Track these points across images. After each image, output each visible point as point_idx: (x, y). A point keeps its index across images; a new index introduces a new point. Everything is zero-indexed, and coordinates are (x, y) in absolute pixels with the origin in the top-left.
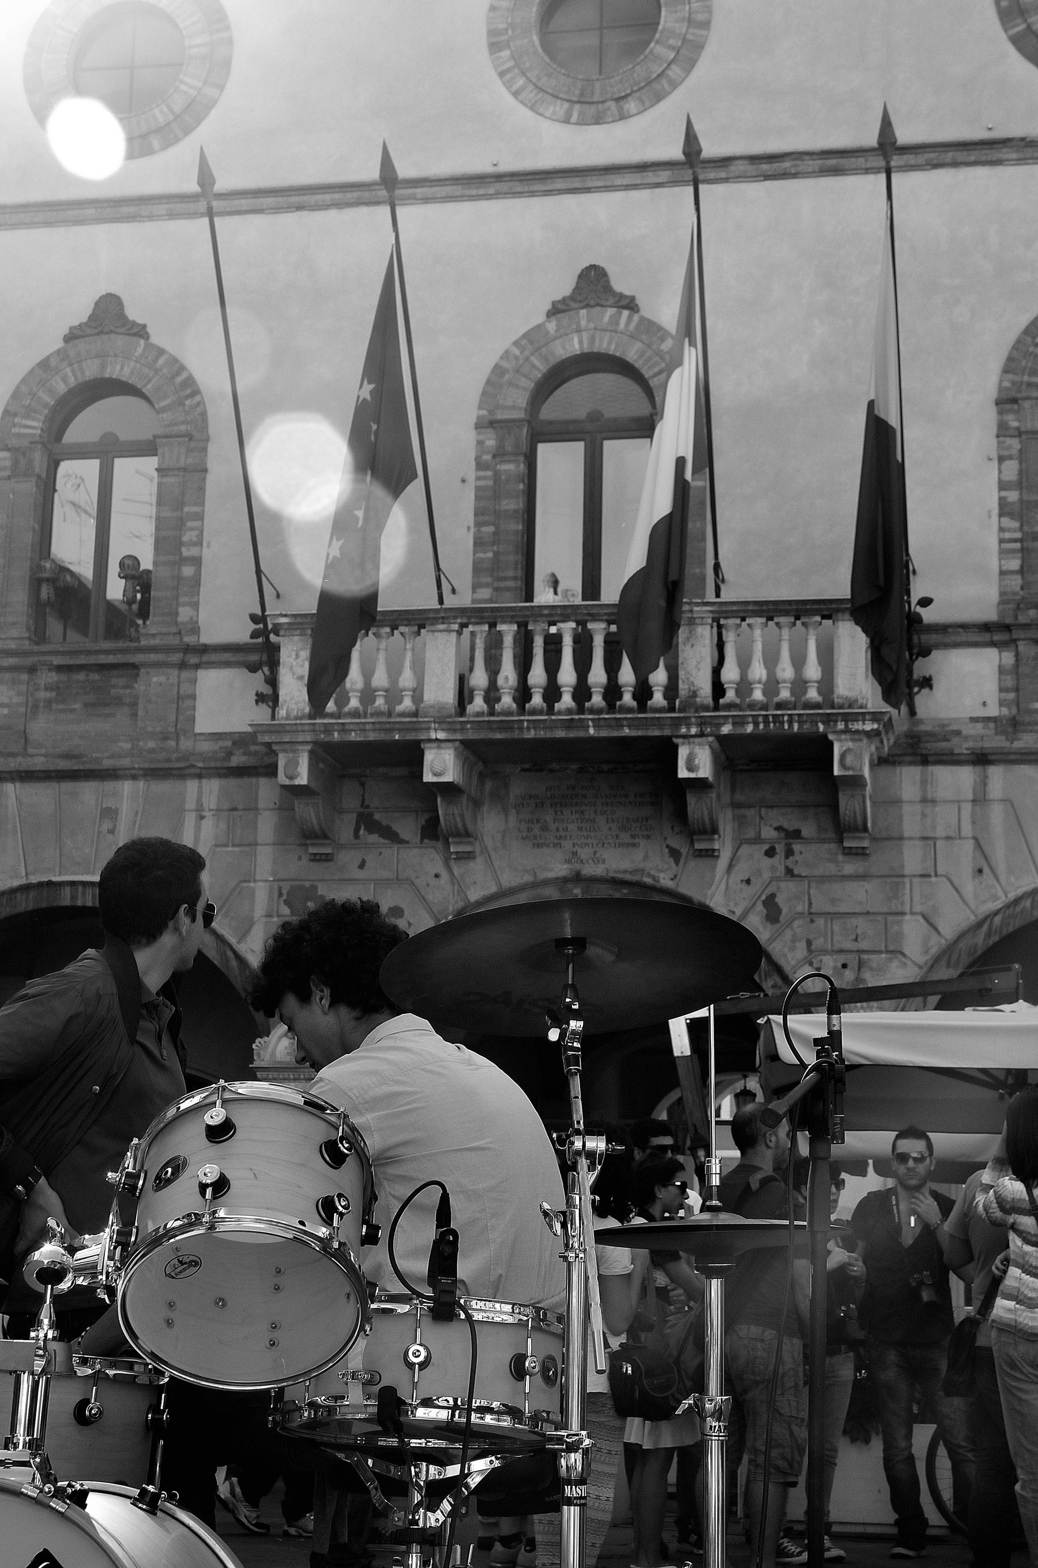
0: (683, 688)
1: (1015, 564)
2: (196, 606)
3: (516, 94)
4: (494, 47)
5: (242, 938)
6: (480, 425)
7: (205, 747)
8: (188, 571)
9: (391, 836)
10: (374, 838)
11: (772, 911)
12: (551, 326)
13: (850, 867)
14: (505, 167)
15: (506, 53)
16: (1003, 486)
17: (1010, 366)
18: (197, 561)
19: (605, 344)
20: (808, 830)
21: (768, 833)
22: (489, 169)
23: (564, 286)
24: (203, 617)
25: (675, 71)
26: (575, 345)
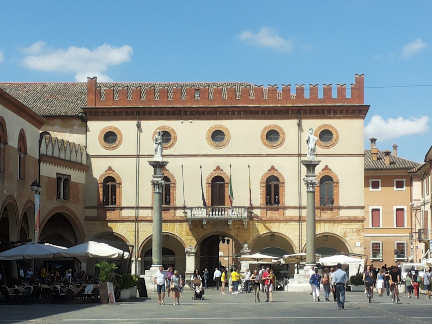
0: (229, 215)
1: (262, 200)
2: (176, 202)
3: (209, 145)
4: (207, 139)
5: (182, 238)
6: (206, 183)
7: (178, 218)
8: (175, 198)
9: (197, 227)
10: (196, 228)
11: (237, 236)
12: (214, 172)
13: (245, 231)
14: (208, 154)
15: (208, 140)
16: (261, 192)
17: (262, 179)
18: (176, 197)
19: (219, 175)
20: (241, 227)
21: (237, 228)
22: (206, 154)
23: (215, 168)
24: (177, 204)
25: (227, 144)
26: (216, 175)
